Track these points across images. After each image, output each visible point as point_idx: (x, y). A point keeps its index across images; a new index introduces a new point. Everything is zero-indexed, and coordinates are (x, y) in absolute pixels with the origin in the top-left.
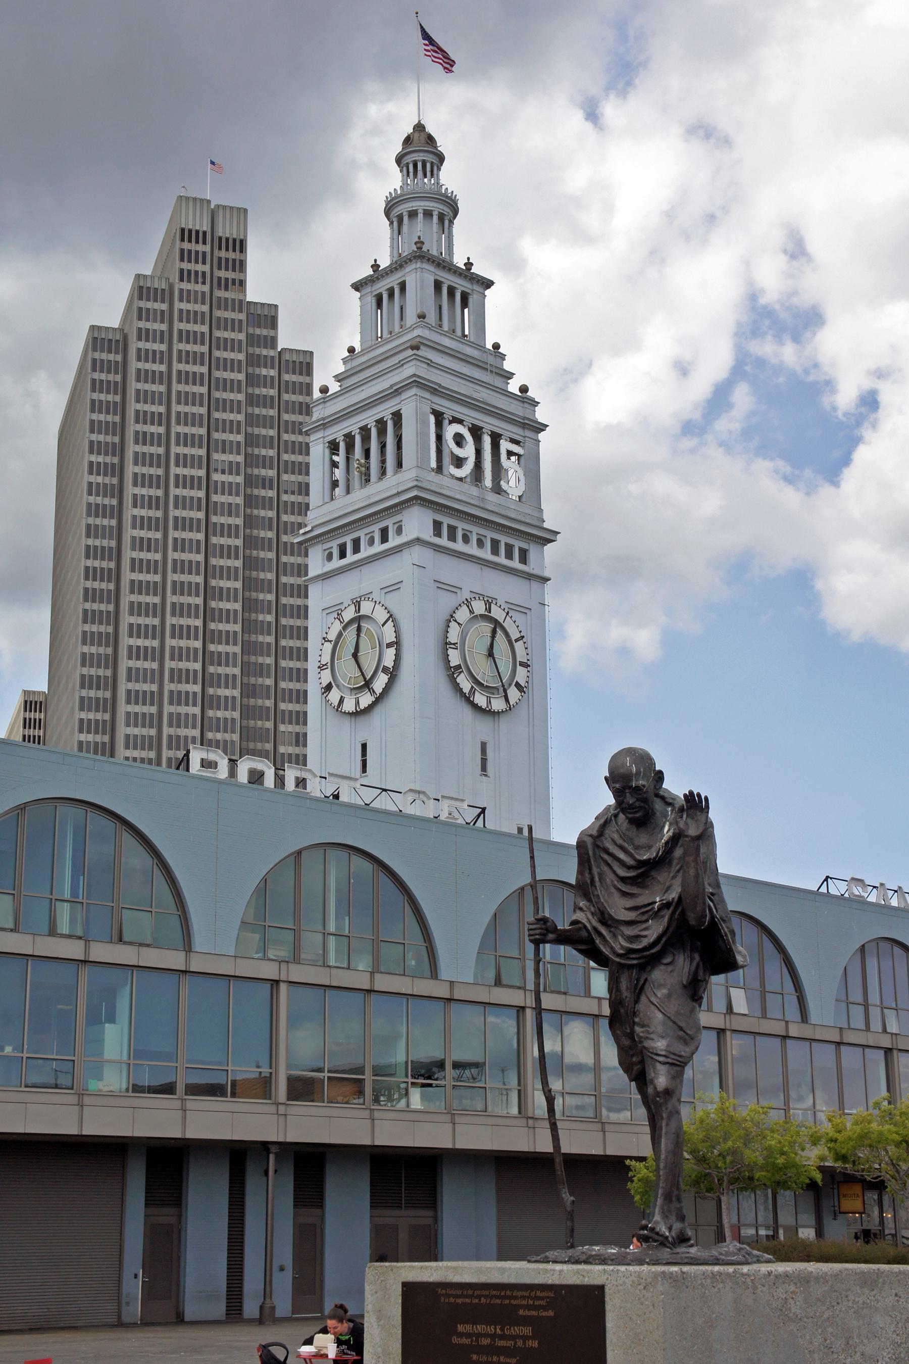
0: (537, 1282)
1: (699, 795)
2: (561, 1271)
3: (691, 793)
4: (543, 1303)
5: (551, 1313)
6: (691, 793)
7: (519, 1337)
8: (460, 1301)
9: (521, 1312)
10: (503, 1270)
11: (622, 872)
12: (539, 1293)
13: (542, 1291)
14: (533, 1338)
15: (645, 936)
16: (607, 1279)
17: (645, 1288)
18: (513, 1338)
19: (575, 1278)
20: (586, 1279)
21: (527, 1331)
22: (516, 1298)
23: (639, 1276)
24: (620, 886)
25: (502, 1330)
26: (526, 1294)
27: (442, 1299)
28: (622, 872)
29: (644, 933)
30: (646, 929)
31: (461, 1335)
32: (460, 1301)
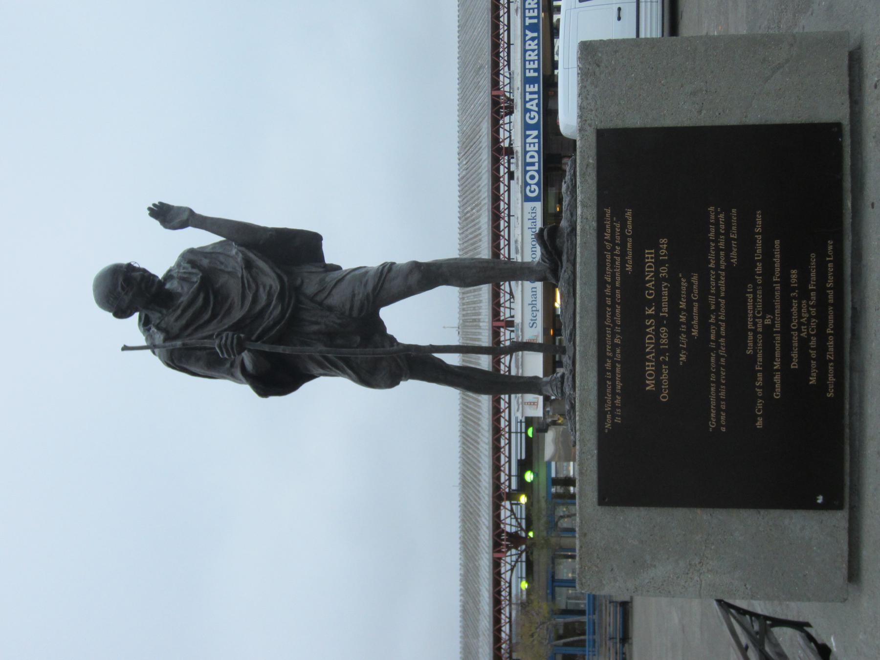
0: (595, 248)
1: (154, 205)
2: (583, 206)
3: (149, 209)
4: (618, 225)
5: (629, 214)
6: (149, 209)
7: (657, 272)
8: (619, 386)
9: (629, 268)
10: (584, 244)
11: (207, 316)
12: (608, 236)
13: (604, 272)
14: (658, 249)
15: (271, 287)
16: (590, 125)
17: (598, 66)
18: (658, 281)
19: (590, 181)
20: (591, 161)
21: (649, 256)
22: (613, 275)
23: (585, 284)
24: (219, 317)
25: (649, 304)
26: (608, 257)
27: (618, 420)
28: (207, 316)
29: (268, 288)
30: (264, 287)
31: (658, 383)
32: (619, 386)
